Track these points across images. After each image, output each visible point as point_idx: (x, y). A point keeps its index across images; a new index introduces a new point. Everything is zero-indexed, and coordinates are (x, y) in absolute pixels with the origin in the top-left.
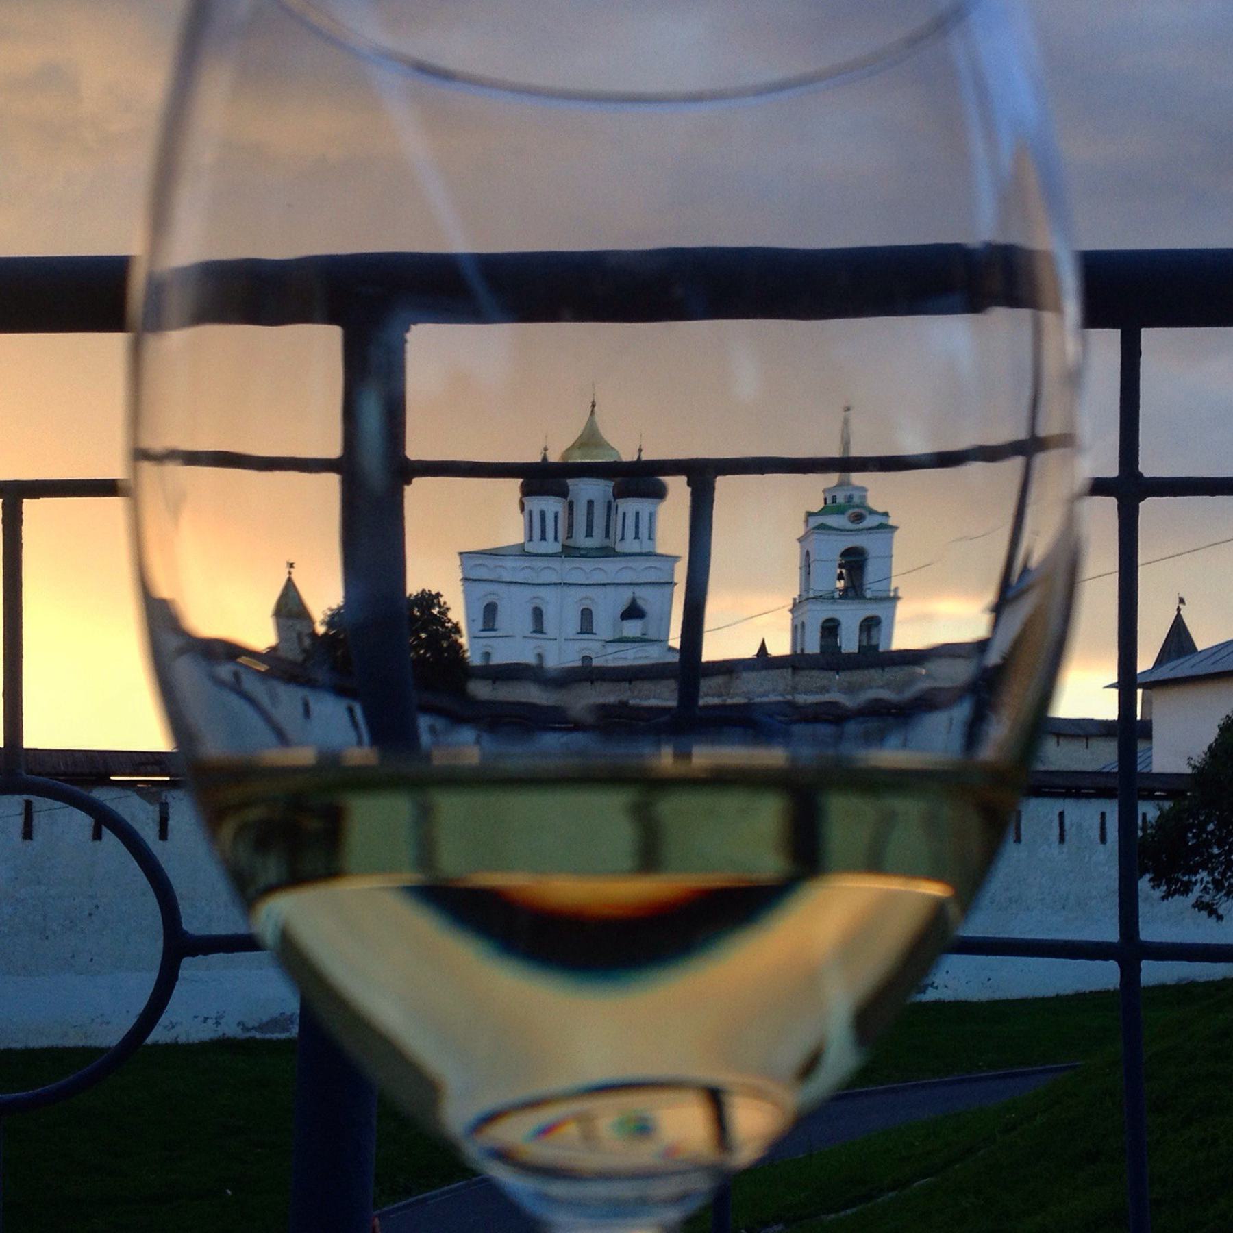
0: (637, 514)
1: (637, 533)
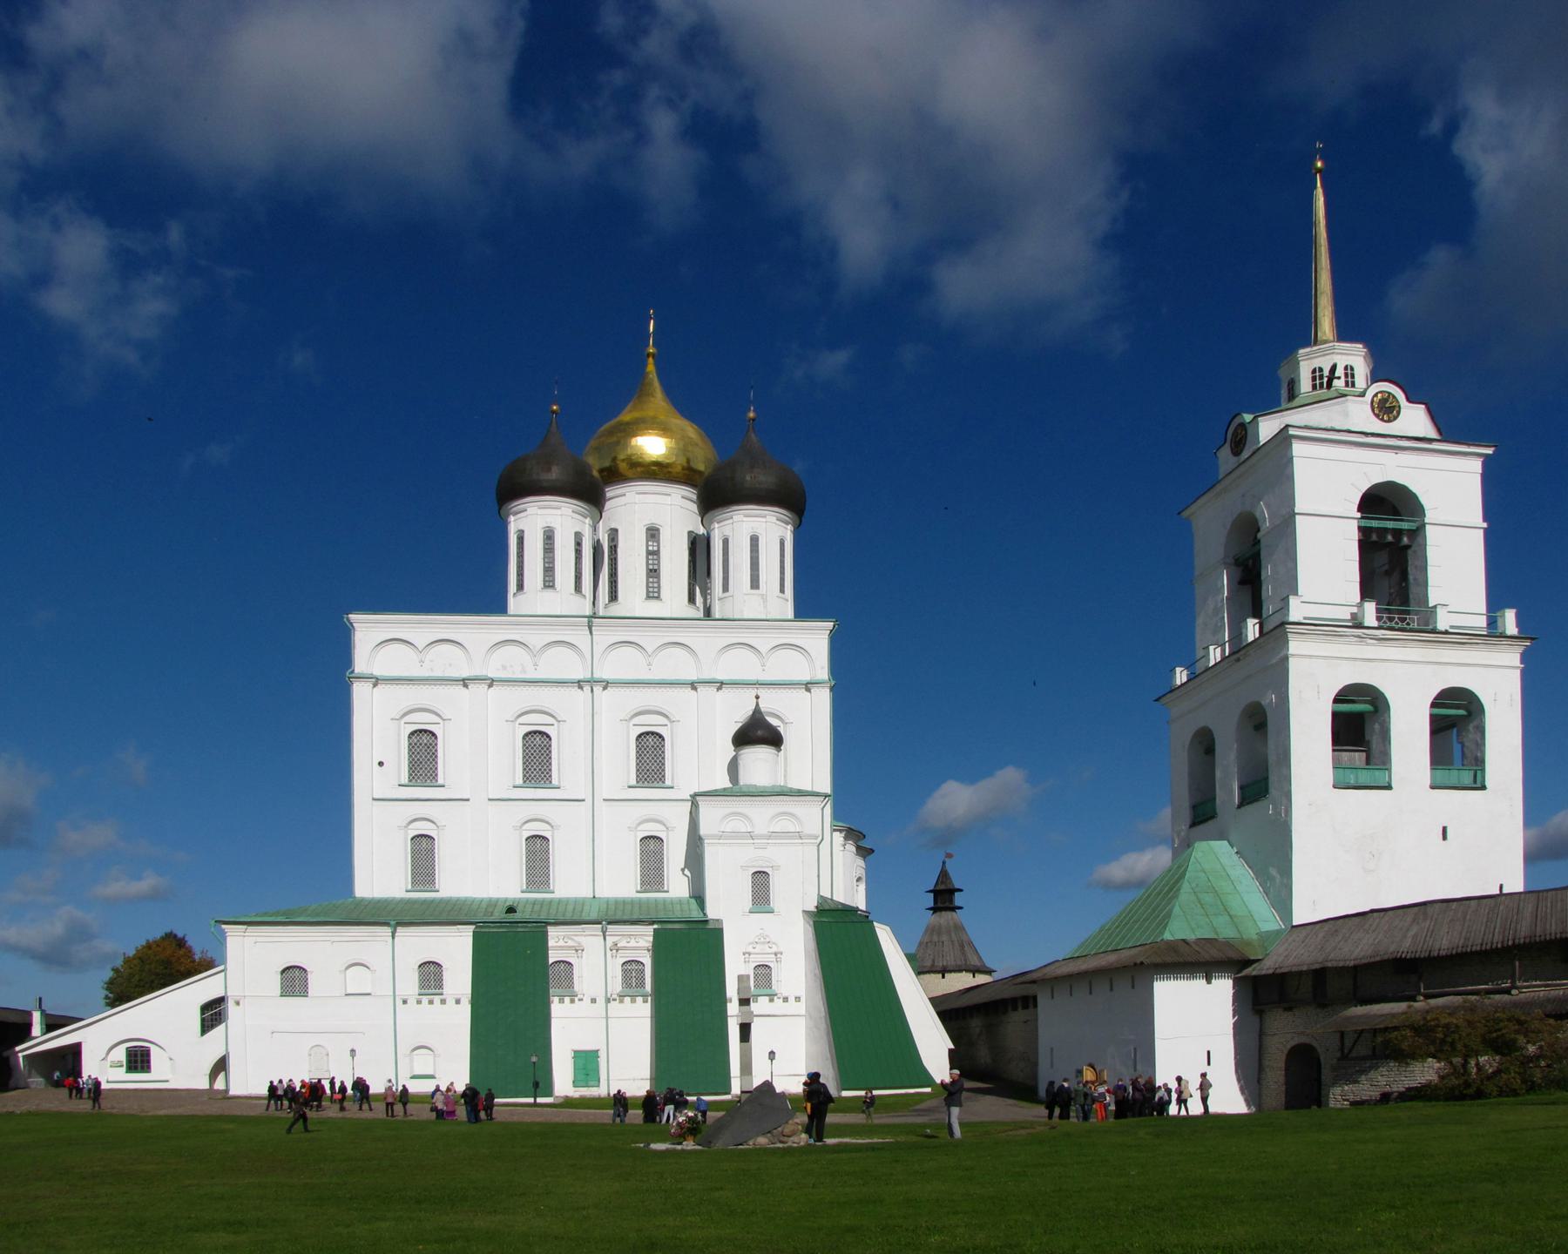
0: (754, 541)
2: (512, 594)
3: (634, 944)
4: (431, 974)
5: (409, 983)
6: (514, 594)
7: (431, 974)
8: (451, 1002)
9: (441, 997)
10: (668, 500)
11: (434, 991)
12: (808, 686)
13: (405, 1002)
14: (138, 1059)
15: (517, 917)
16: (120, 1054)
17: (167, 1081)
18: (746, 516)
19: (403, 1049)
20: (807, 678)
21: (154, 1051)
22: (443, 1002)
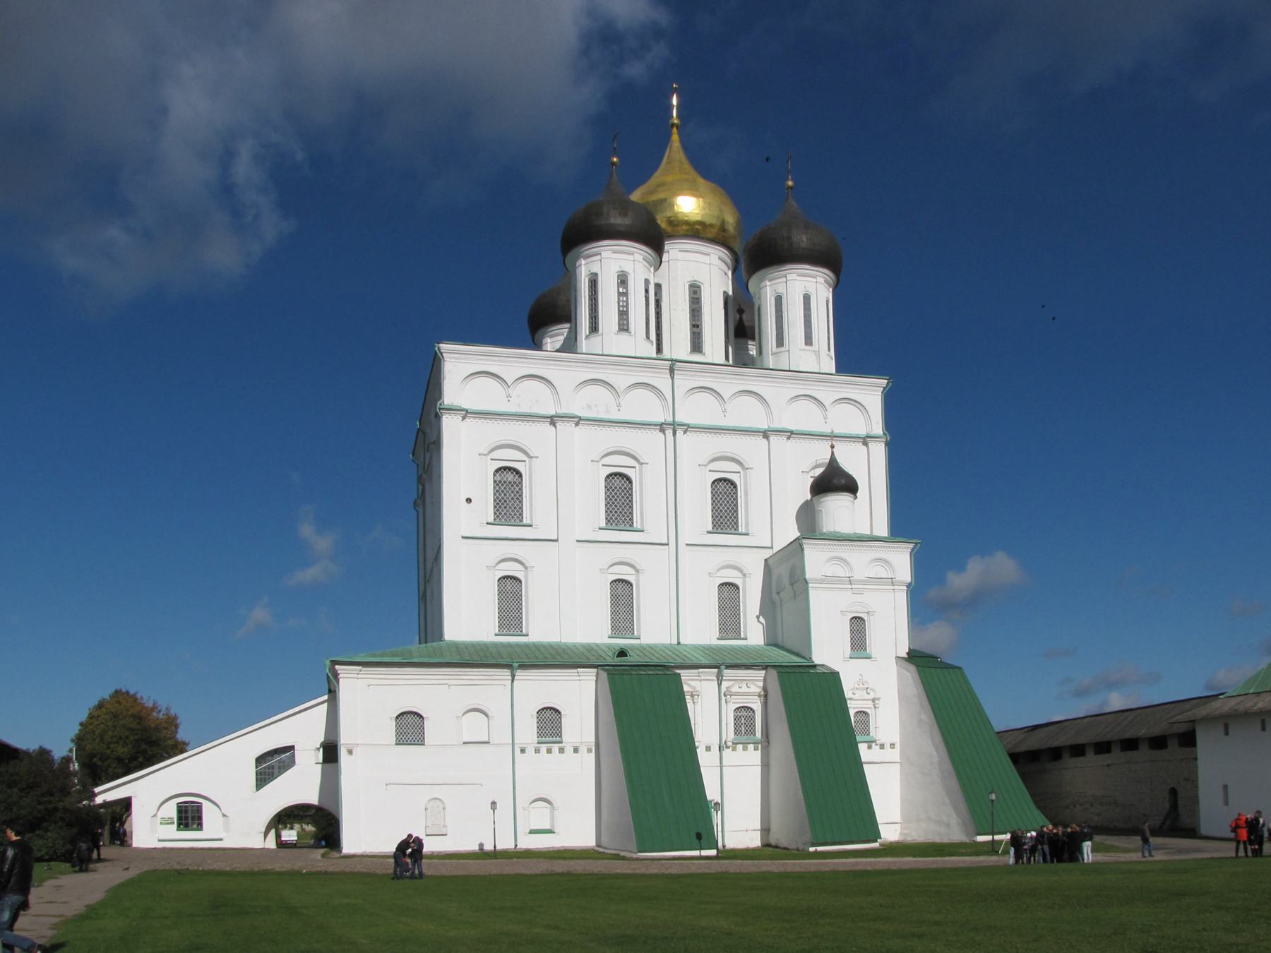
3: (744, 689)
4: (550, 721)
5: (528, 731)
7: (550, 721)
9: (560, 745)
10: (706, 259)
11: (551, 739)
12: (865, 440)
13: (523, 751)
14: (189, 816)
15: (631, 659)
16: (171, 811)
17: (221, 840)
19: (523, 800)
20: (863, 432)
21: (207, 809)
22: (562, 750)
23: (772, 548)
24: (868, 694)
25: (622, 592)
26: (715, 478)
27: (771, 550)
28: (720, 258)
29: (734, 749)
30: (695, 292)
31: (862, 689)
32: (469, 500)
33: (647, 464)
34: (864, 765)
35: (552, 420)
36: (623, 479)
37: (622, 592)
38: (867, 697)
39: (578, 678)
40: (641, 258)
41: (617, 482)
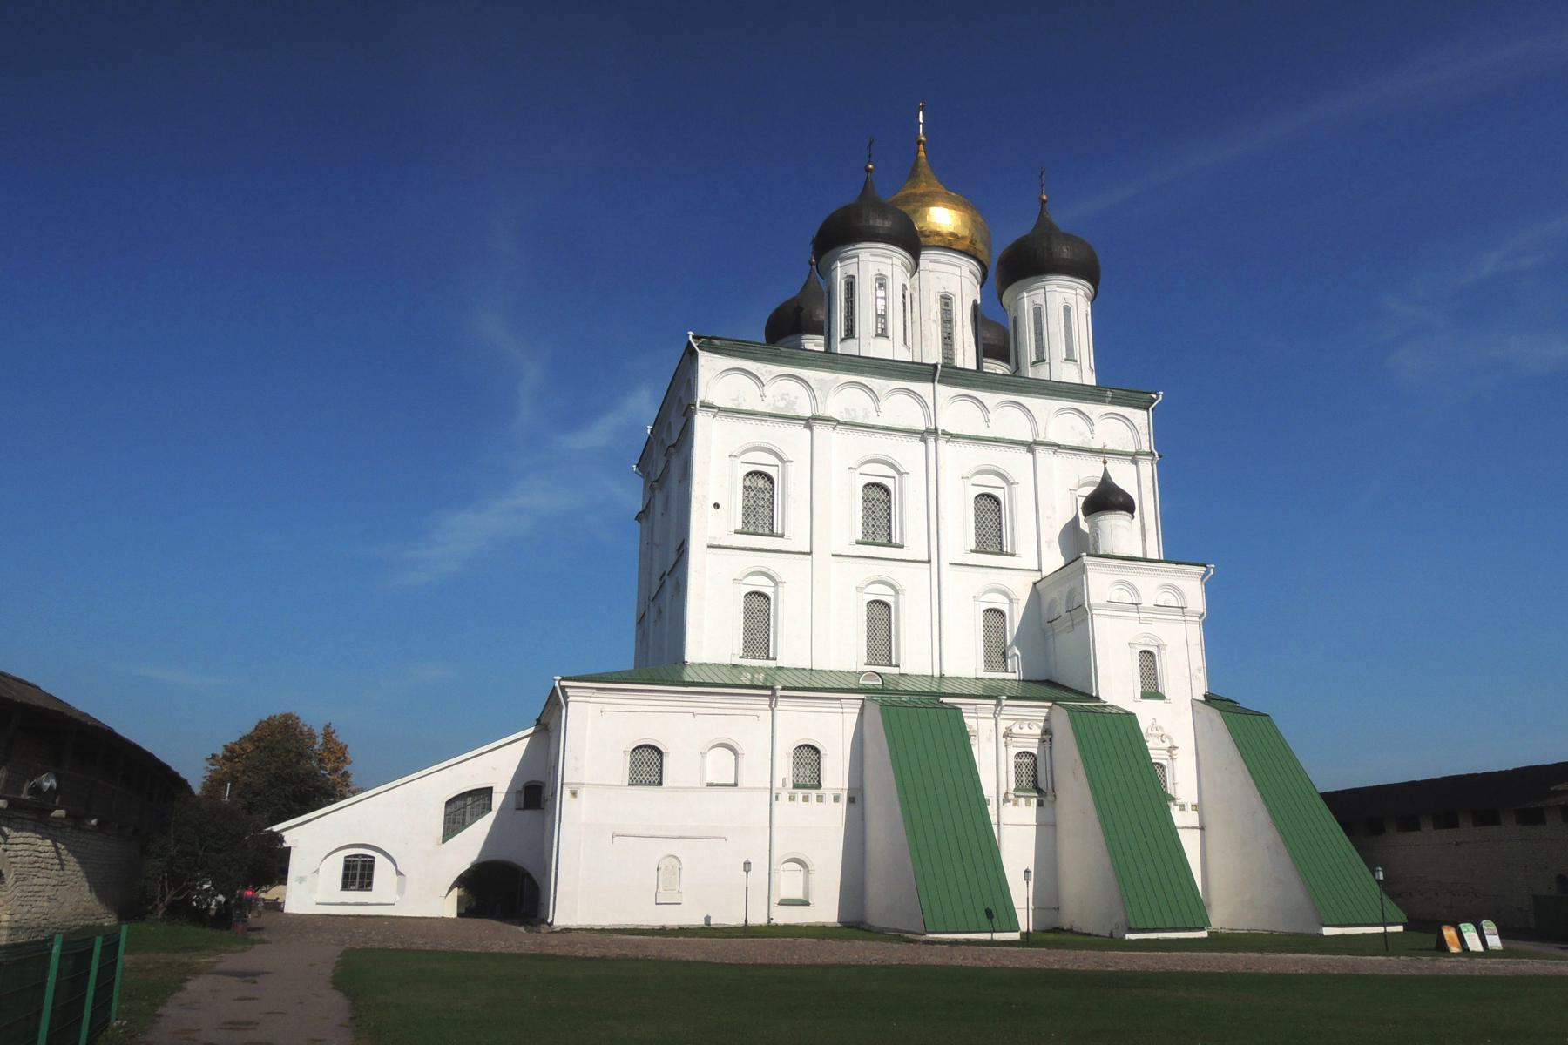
0: (1067, 310)
1: (1070, 349)
2: (839, 340)
3: (1026, 730)
6: (843, 340)
8: (829, 798)
18: (1058, 286)
20: (1133, 450)
22: (820, 798)
23: (1040, 570)
24: (1163, 742)
25: (881, 615)
26: (978, 493)
27: (1039, 574)
28: (970, 272)
29: (1016, 804)
30: (946, 300)
31: (1156, 736)
32: (717, 506)
33: (908, 473)
34: (1179, 830)
35: (809, 422)
36: (881, 489)
37: (881, 615)
38: (1162, 745)
39: (841, 710)
40: (899, 263)
41: (877, 494)
